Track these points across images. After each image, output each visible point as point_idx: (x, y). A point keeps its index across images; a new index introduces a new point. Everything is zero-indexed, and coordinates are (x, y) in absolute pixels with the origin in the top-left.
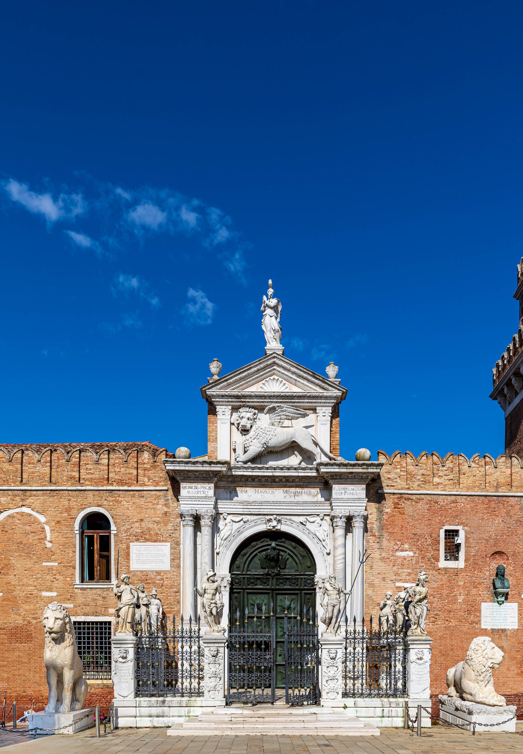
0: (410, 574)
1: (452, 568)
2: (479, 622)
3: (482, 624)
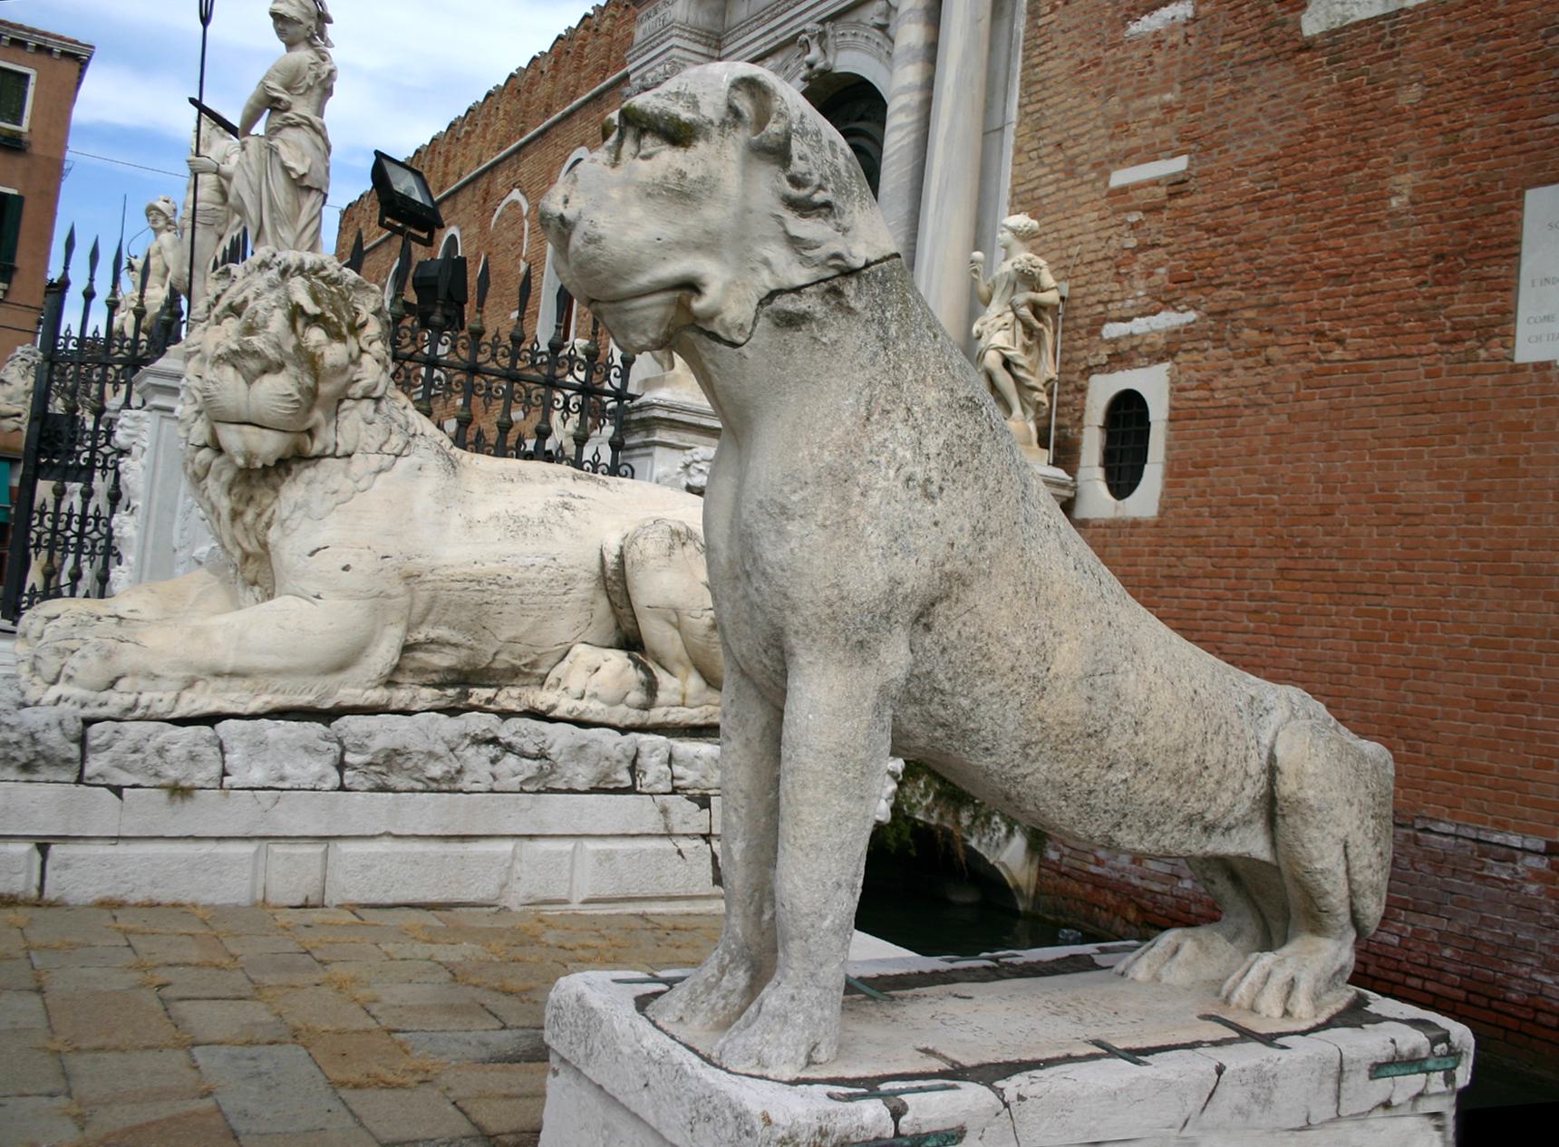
0: (1169, 109)
1: (1369, 22)
2: (1501, 323)
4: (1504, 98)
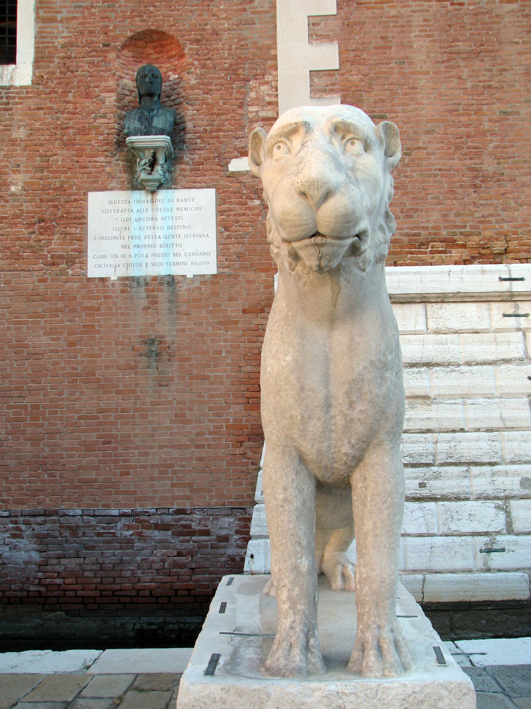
2: (79, 256)
3: (91, 262)
4: (74, 144)
